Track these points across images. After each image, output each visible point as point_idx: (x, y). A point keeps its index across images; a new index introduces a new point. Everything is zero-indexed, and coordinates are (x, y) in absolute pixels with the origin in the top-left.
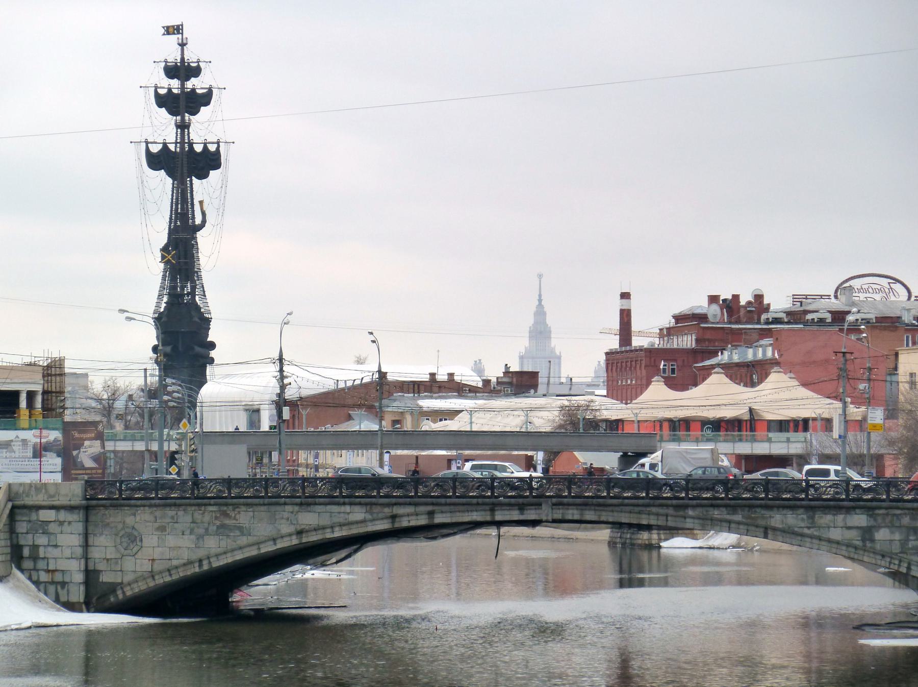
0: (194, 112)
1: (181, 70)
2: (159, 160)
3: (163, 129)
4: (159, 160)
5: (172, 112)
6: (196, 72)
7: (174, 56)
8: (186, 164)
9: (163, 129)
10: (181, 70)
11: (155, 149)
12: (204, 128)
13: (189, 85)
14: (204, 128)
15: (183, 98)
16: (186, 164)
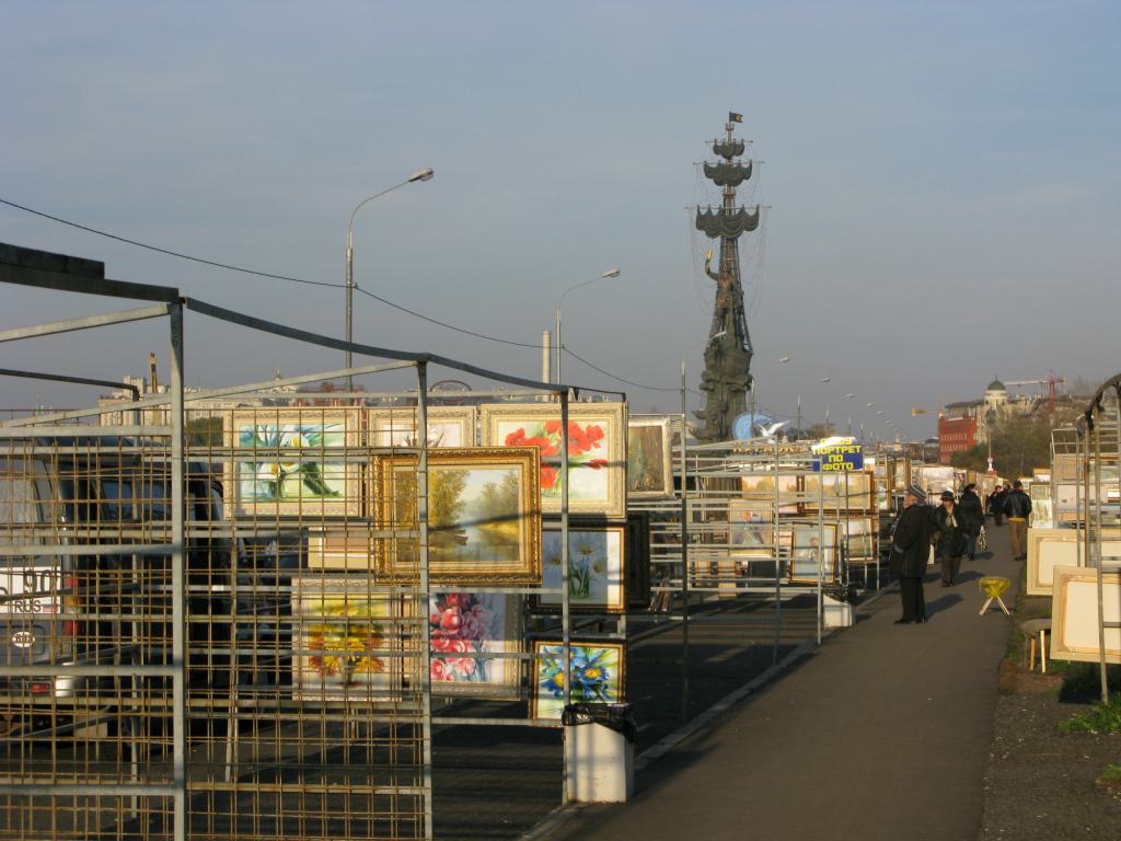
0: (738, 182)
1: (730, 150)
2: (706, 223)
3: (711, 196)
4: (706, 223)
5: (719, 183)
6: (738, 149)
7: (722, 137)
8: (727, 226)
9: (711, 196)
10: (730, 150)
11: (703, 212)
12: (746, 196)
13: (735, 159)
14: (746, 196)
15: (728, 170)
16: (727, 226)
